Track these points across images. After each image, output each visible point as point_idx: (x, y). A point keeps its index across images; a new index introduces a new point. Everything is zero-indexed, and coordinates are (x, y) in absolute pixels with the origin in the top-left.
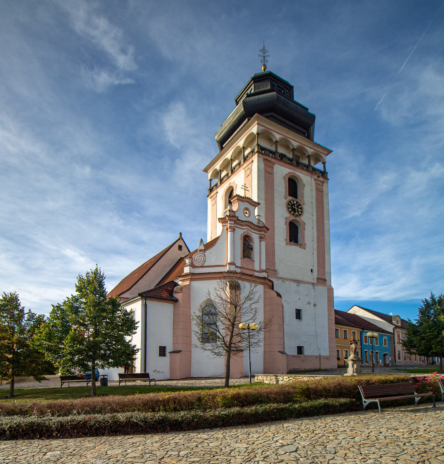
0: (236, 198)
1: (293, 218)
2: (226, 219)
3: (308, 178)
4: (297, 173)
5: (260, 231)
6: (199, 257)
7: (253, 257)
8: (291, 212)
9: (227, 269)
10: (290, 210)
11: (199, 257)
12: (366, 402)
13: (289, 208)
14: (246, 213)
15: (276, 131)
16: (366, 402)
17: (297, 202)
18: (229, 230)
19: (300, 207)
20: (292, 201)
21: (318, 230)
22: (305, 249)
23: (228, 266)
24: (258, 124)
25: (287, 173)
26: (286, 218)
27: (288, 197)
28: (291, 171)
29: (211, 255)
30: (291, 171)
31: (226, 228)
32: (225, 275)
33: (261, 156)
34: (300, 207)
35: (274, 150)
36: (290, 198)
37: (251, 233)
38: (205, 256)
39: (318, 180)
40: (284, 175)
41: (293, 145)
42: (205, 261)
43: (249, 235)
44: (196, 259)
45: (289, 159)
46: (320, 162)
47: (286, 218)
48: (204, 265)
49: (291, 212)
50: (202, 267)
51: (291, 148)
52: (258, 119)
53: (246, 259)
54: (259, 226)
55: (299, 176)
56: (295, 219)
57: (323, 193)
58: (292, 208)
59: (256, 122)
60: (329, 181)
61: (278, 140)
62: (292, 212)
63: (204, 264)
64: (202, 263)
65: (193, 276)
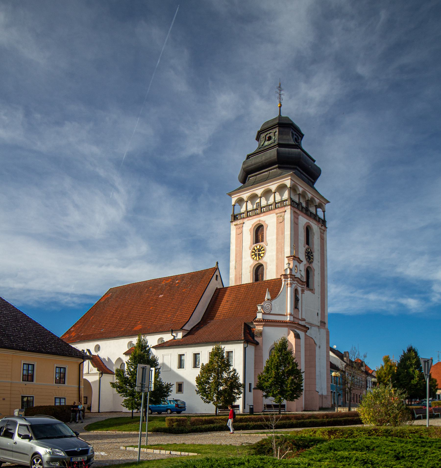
0: (292, 258)
1: (308, 265)
2: (288, 276)
3: (316, 226)
4: (311, 223)
5: (302, 285)
6: (267, 306)
7: (299, 307)
9: (288, 319)
10: (307, 257)
11: (267, 306)
12: (417, 416)
13: (306, 256)
14: (296, 270)
15: (300, 185)
16: (417, 416)
18: (289, 286)
19: (312, 254)
22: (314, 294)
23: (288, 316)
24: (291, 179)
25: (305, 223)
27: (306, 245)
28: (308, 221)
29: (276, 305)
31: (287, 284)
32: (288, 324)
33: (292, 208)
34: (312, 254)
35: (298, 201)
37: (298, 287)
38: (271, 305)
39: (322, 229)
40: (304, 225)
41: (308, 197)
42: (271, 309)
43: (297, 288)
44: (265, 308)
45: (302, 207)
46: (321, 208)
48: (271, 313)
50: (269, 314)
51: (307, 199)
52: (291, 175)
53: (296, 310)
54: (301, 281)
56: (309, 265)
57: (324, 240)
58: (308, 256)
59: (290, 178)
60: (327, 229)
61: (301, 193)
62: (308, 260)
63: (270, 312)
64: (269, 311)
65: (266, 323)
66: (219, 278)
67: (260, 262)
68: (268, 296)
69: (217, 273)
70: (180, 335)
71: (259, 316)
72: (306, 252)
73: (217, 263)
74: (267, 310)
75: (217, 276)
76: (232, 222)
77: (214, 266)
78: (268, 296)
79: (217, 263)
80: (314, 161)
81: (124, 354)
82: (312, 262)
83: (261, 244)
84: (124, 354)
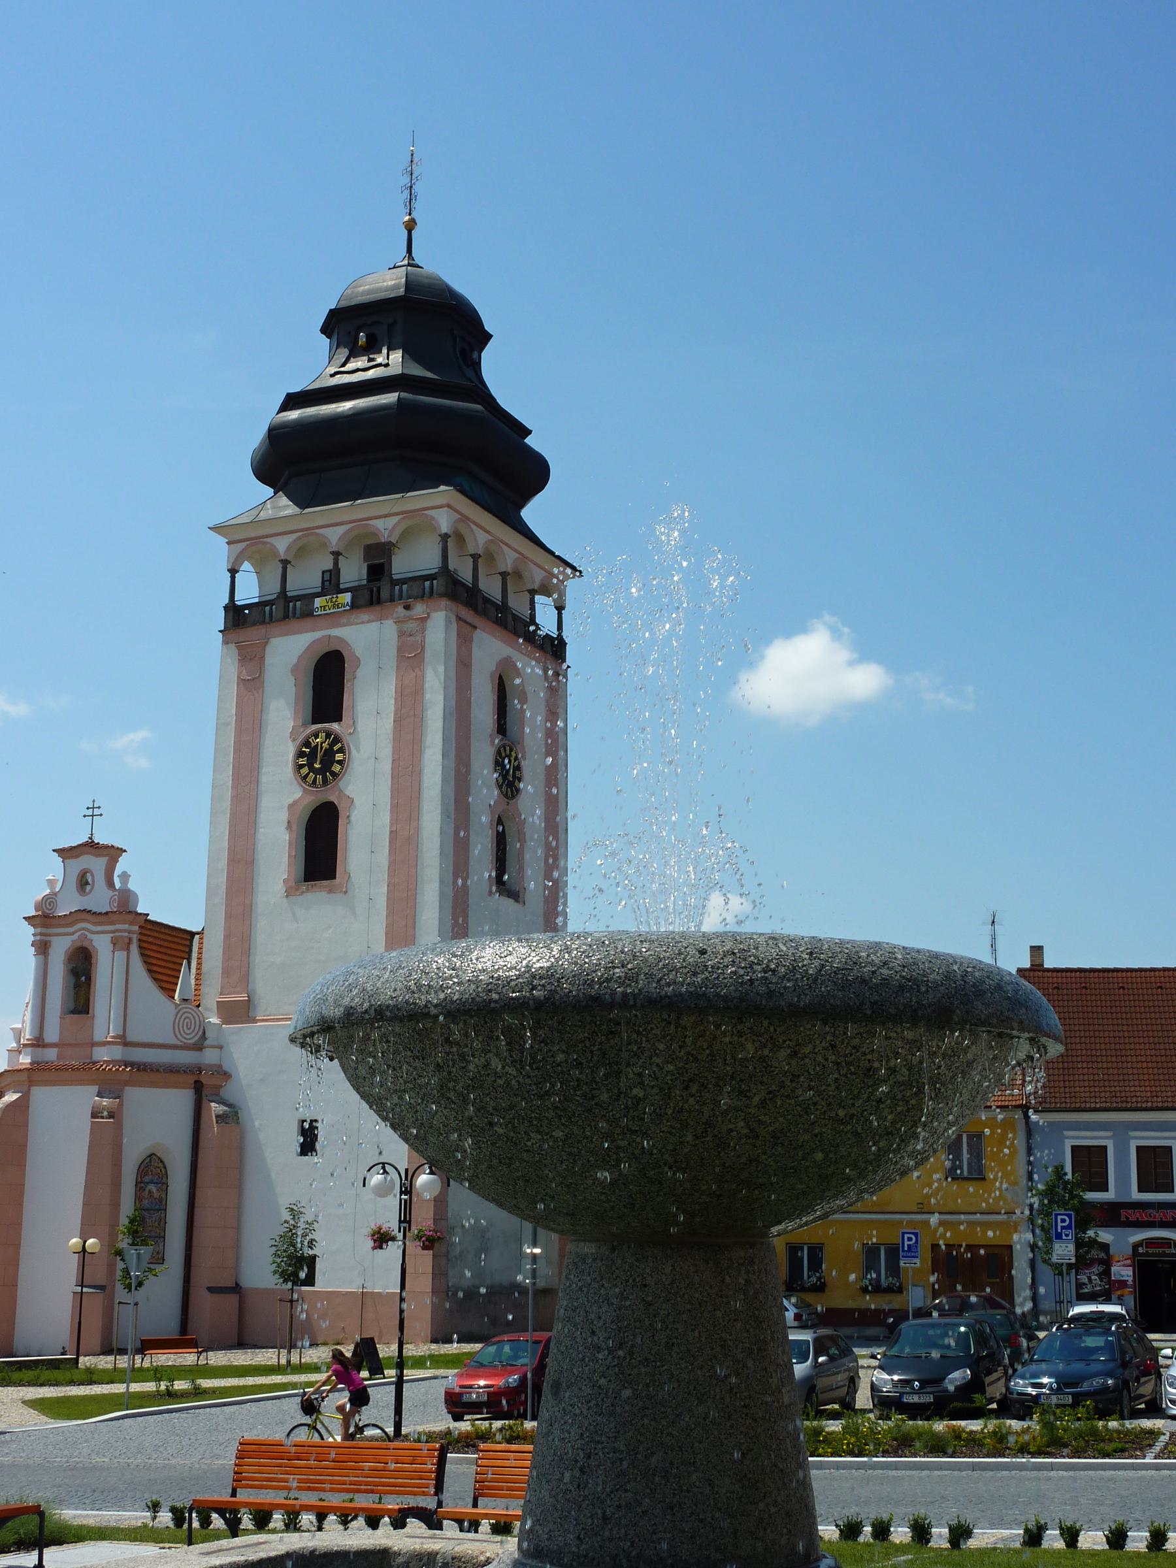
4: (336, 632)
17: (328, 735)
21: (395, 807)
26: (291, 807)
28: (317, 635)
30: (317, 635)
40: (295, 660)
55: (340, 640)
72: (301, 754)
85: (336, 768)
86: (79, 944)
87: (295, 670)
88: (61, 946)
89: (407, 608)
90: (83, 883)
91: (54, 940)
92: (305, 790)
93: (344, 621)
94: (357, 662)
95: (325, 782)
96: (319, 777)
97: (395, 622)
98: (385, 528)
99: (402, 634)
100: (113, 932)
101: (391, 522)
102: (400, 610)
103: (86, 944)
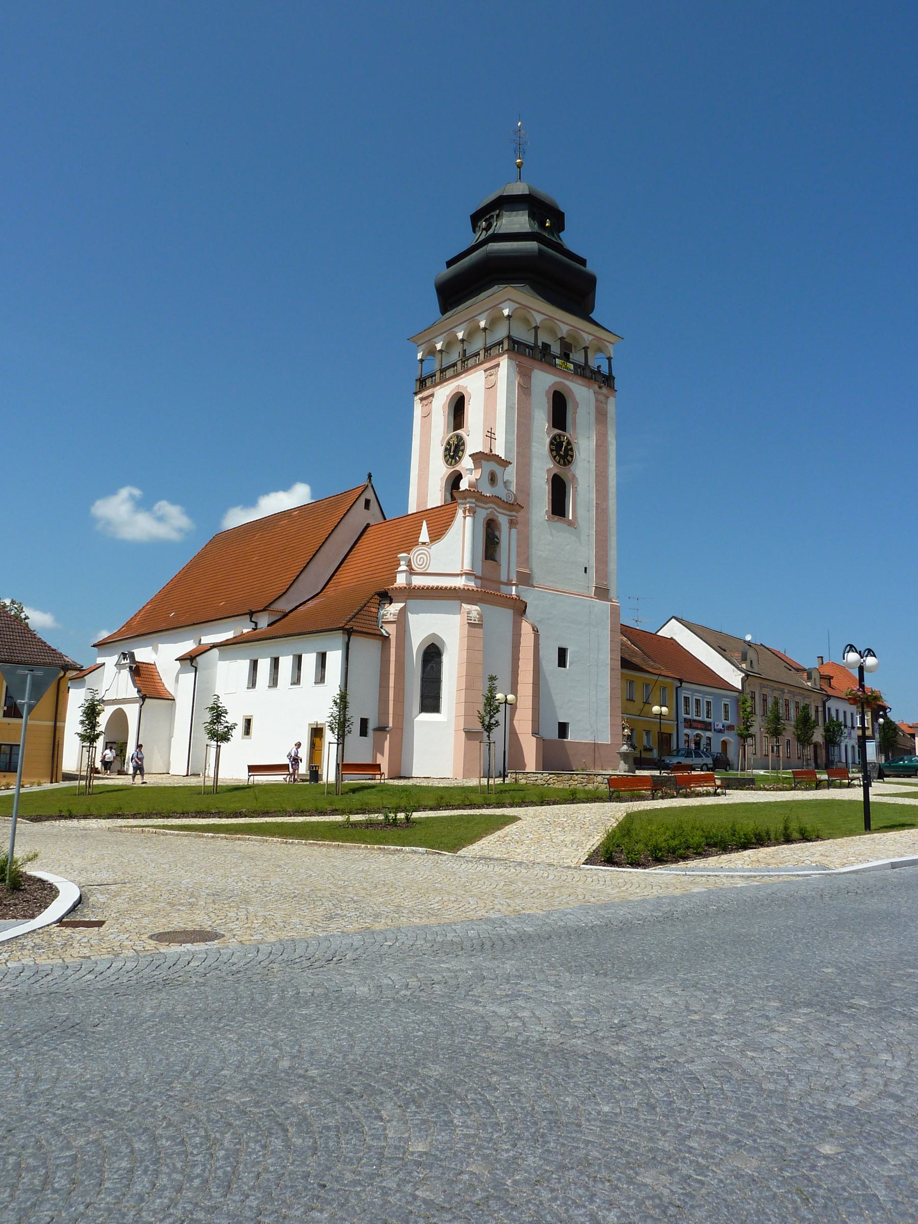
8: (554, 457)
20: (557, 437)
26: (548, 471)
27: (552, 429)
28: (558, 379)
36: (557, 431)
40: (547, 388)
47: (548, 471)
49: (555, 457)
66: (373, 504)
67: (457, 468)
68: (424, 536)
69: (369, 494)
70: (264, 621)
71: (401, 580)
73: (370, 476)
74: (421, 565)
75: (367, 503)
76: (416, 394)
77: (365, 482)
78: (424, 536)
79: (370, 476)
80: (583, 262)
81: (176, 660)
82: (570, 462)
83: (459, 431)
84: (176, 660)
85: (569, 458)
86: (491, 517)
87: (547, 393)
88: (483, 514)
89: (600, 388)
90: (493, 479)
91: (478, 509)
92: (554, 464)
93: (570, 378)
94: (576, 405)
95: (565, 465)
96: (562, 461)
97: (595, 393)
98: (587, 338)
99: (597, 400)
100: (511, 516)
101: (591, 338)
102: (596, 387)
103: (495, 518)
